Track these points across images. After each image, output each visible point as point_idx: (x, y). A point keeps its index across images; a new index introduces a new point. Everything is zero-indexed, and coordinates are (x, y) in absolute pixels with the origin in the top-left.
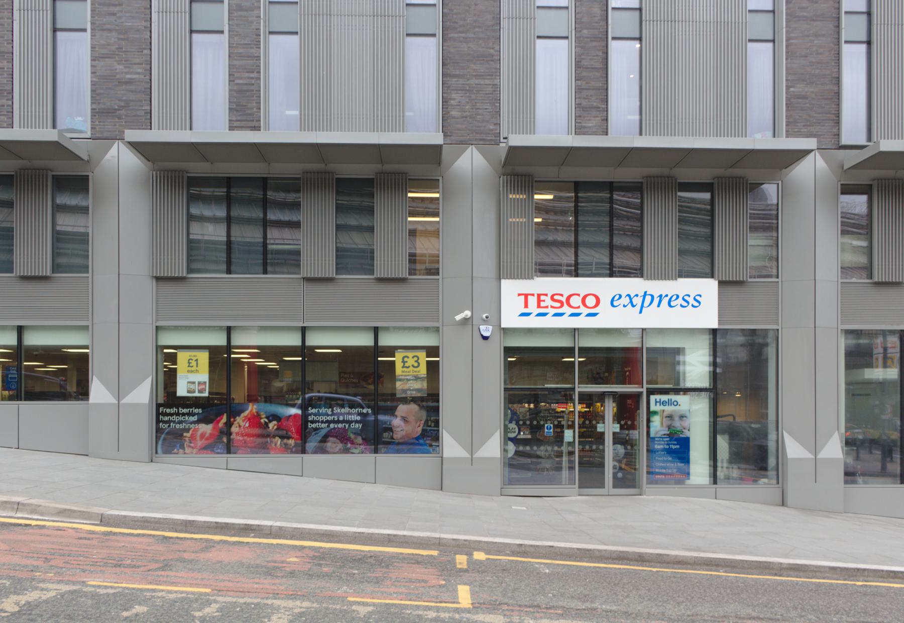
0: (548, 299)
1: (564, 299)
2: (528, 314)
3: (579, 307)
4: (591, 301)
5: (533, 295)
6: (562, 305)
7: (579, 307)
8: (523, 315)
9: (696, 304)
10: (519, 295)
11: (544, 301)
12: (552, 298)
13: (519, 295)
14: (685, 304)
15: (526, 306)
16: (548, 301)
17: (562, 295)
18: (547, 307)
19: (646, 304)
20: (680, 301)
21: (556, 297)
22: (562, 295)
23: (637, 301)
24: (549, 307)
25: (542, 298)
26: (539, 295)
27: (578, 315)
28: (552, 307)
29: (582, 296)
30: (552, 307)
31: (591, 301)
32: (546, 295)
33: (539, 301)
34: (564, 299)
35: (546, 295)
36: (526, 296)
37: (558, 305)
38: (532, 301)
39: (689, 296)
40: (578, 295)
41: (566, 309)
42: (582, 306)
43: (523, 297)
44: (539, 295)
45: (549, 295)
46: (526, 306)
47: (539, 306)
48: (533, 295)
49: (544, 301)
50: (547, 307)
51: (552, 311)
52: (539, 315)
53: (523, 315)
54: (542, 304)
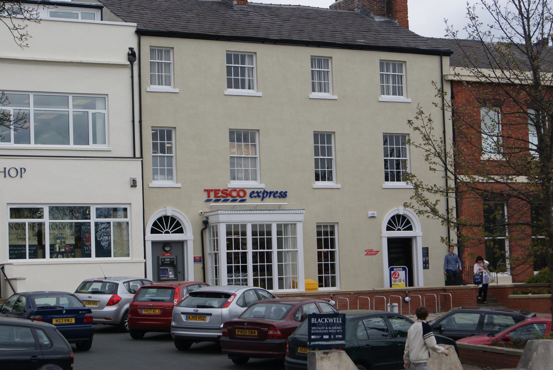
0: (220, 192)
1: (228, 192)
7: (235, 197)
9: (284, 196)
14: (280, 196)
15: (209, 196)
16: (220, 194)
18: (219, 197)
19: (265, 196)
20: (278, 194)
23: (261, 194)
25: (218, 192)
31: (242, 194)
39: (282, 192)
41: (229, 198)
46: (209, 196)
47: (215, 196)
48: (212, 190)
49: (218, 193)
51: (222, 199)
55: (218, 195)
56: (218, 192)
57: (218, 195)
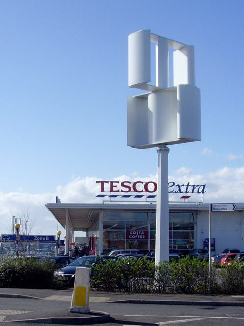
0: (119, 185)
1: (131, 186)
2: (103, 196)
3: (142, 191)
5: (107, 182)
6: (130, 190)
7: (142, 191)
8: (99, 196)
10: (98, 182)
11: (116, 187)
12: (123, 185)
13: (98, 182)
15: (102, 190)
17: (130, 183)
18: (118, 191)
21: (125, 184)
22: (130, 183)
25: (115, 184)
26: (112, 183)
27: (141, 196)
28: (122, 191)
29: (144, 184)
30: (122, 191)
32: (118, 182)
33: (112, 187)
34: (131, 186)
35: (118, 182)
36: (102, 183)
37: (127, 189)
40: (142, 183)
41: (133, 193)
42: (144, 190)
44: (112, 183)
45: (120, 183)
46: (102, 190)
47: (112, 190)
48: (107, 182)
49: (116, 187)
50: (118, 191)
52: (111, 196)
53: (99, 196)
54: (115, 189)
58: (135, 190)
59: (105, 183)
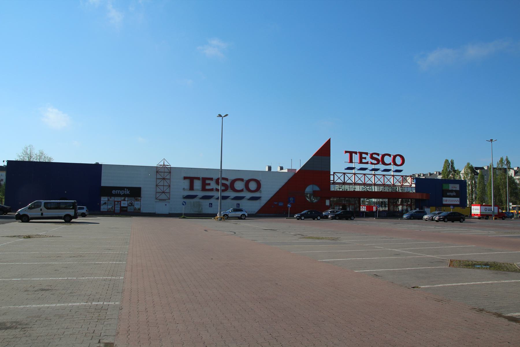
1: (379, 158)
4: (398, 160)
6: (378, 163)
10: (346, 152)
11: (365, 158)
12: (372, 157)
13: (346, 152)
15: (351, 161)
18: (367, 163)
22: (378, 155)
24: (369, 163)
25: (364, 156)
30: (372, 163)
31: (398, 160)
32: (367, 154)
33: (361, 158)
34: (379, 158)
36: (351, 153)
38: (356, 158)
40: (390, 155)
41: (381, 167)
43: (348, 154)
44: (361, 154)
46: (351, 161)
47: (361, 162)
48: (356, 153)
49: (365, 158)
50: (367, 163)
55: (364, 161)
56: (364, 156)
57: (364, 161)
58: (384, 163)
59: (353, 154)
